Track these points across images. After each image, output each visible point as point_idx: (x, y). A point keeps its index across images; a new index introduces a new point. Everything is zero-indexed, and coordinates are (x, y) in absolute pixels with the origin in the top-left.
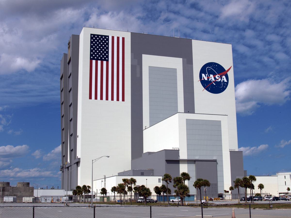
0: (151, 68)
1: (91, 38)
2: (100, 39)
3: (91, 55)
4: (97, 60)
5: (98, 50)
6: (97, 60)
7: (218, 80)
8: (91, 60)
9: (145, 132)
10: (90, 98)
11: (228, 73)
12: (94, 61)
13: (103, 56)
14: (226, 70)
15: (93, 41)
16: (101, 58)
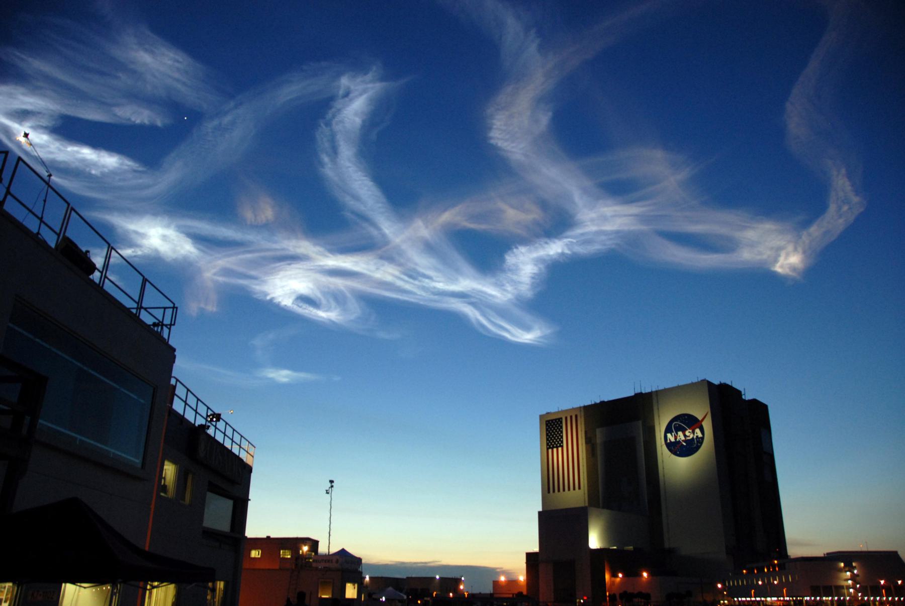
1: (547, 425)
3: (547, 444)
4: (552, 449)
8: (548, 449)
10: (549, 492)
11: (704, 424)
12: (550, 451)
14: (700, 419)
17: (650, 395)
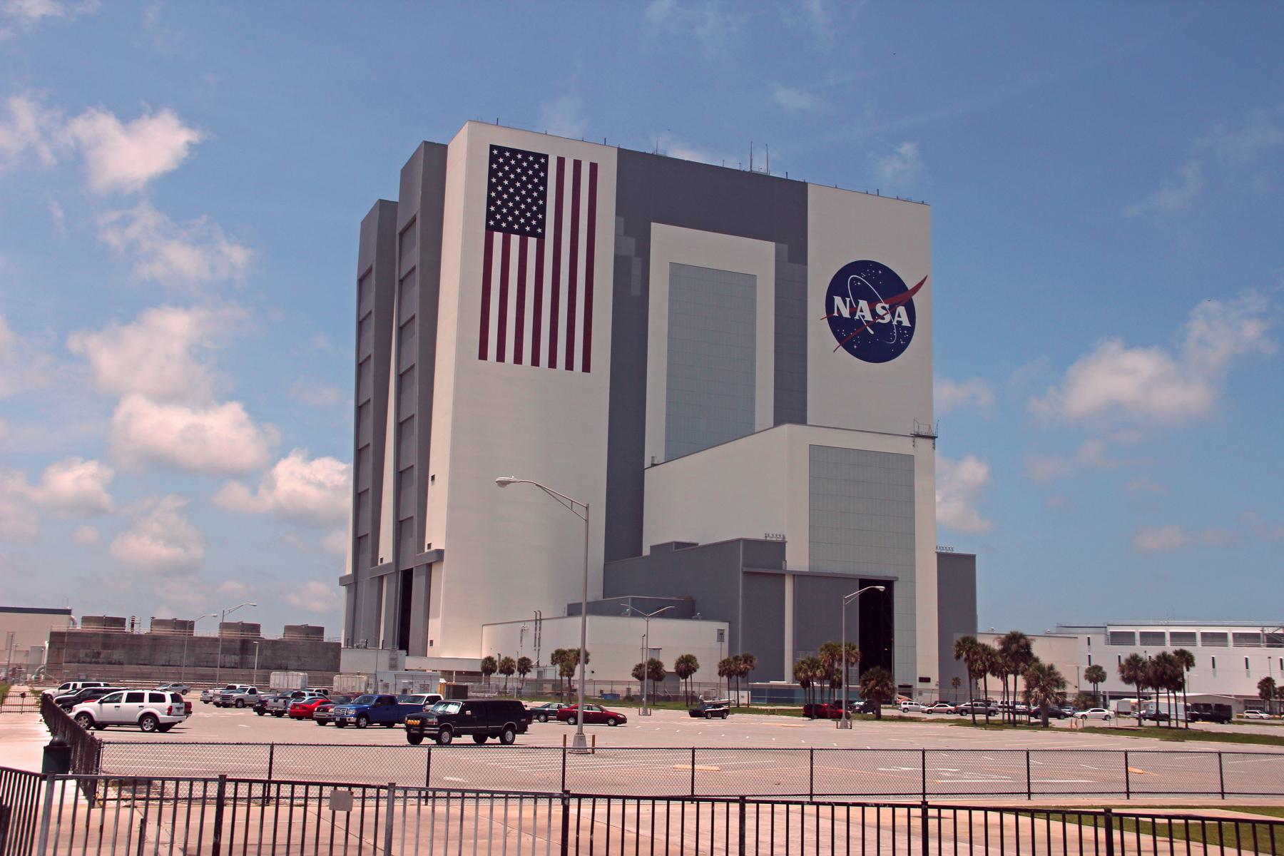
0: (676, 270)
1: (493, 159)
2: (519, 163)
3: (490, 216)
4: (507, 232)
5: (514, 201)
6: (507, 232)
8: (490, 231)
9: (649, 474)
10: (483, 355)
11: (914, 298)
12: (498, 236)
13: (528, 221)
15: (497, 171)
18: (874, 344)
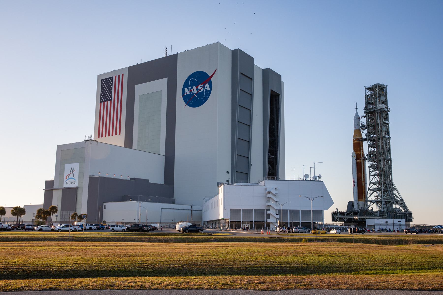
2: (107, 81)
4: (104, 102)
6: (105, 101)
7: (200, 90)
8: (101, 102)
12: (102, 103)
13: (108, 97)
16: (107, 99)
17: (176, 55)
18: (195, 101)
